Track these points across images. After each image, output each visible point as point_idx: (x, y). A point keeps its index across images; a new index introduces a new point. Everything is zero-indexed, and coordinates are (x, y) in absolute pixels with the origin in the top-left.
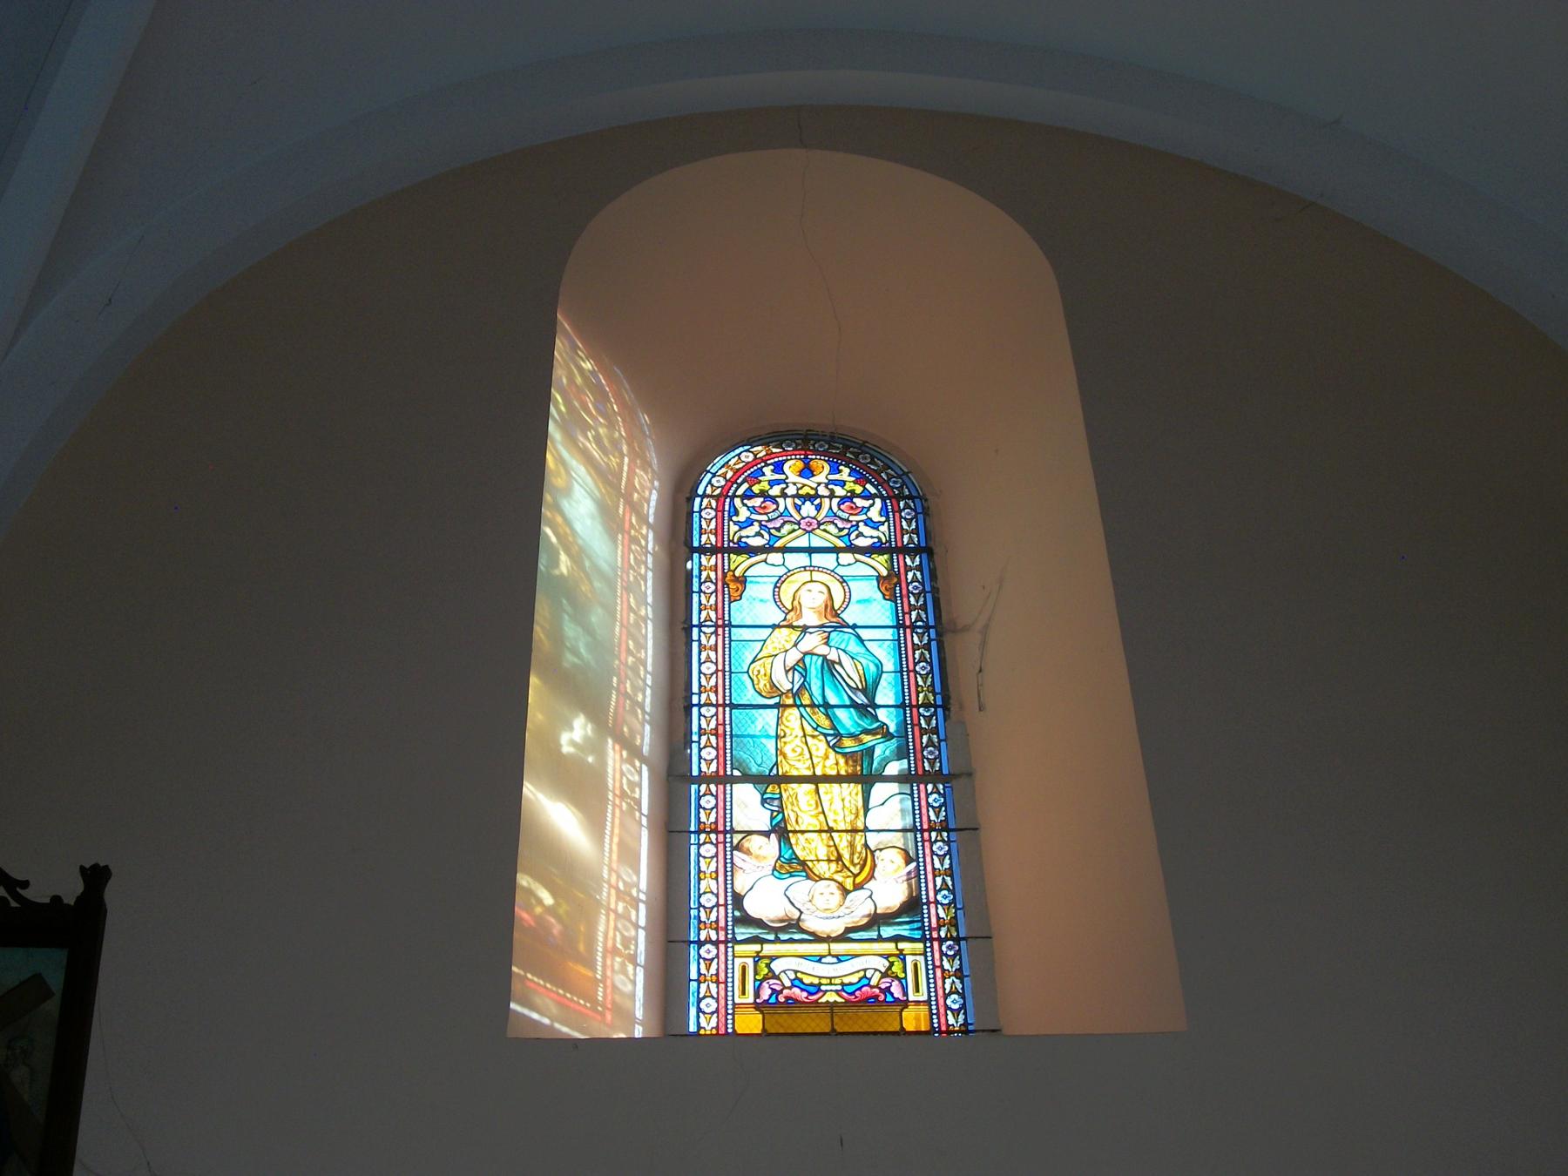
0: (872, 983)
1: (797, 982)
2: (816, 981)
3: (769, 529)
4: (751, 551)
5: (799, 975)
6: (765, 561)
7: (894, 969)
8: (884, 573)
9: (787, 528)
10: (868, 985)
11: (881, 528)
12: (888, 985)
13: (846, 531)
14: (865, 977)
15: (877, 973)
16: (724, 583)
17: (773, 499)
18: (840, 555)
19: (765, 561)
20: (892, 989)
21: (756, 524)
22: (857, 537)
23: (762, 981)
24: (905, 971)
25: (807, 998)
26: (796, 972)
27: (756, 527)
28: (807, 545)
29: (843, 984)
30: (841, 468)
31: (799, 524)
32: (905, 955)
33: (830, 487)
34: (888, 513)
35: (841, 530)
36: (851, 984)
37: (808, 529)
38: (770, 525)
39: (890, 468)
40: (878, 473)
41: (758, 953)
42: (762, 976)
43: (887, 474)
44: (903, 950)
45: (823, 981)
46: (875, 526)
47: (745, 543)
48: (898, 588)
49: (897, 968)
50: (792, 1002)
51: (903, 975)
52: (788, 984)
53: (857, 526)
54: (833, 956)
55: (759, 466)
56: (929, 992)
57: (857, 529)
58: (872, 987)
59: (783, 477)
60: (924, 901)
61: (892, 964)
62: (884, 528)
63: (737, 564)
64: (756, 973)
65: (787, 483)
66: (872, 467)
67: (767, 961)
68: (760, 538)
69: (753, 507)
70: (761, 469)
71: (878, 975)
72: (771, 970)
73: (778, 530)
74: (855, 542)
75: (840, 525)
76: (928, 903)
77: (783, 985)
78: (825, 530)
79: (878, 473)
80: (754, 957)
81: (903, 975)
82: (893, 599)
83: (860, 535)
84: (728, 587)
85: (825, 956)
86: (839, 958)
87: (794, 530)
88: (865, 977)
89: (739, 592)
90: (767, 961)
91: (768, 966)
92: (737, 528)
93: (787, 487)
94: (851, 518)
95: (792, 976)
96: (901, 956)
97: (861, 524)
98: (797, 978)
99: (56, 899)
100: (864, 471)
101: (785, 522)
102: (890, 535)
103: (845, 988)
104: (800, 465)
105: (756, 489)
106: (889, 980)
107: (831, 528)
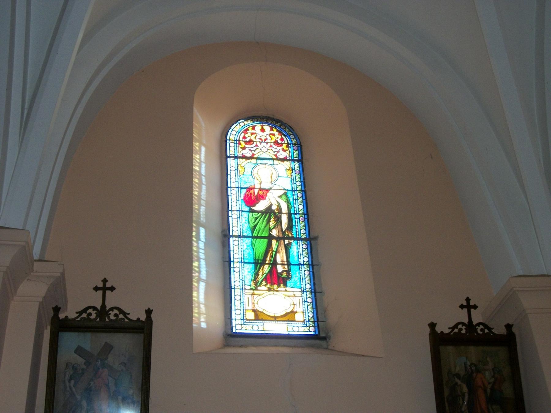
35: (274, 152)
38: (252, 149)
46: (285, 151)
73: (255, 151)
78: (269, 152)
93: (257, 135)
99: (442, 332)
100: (282, 131)
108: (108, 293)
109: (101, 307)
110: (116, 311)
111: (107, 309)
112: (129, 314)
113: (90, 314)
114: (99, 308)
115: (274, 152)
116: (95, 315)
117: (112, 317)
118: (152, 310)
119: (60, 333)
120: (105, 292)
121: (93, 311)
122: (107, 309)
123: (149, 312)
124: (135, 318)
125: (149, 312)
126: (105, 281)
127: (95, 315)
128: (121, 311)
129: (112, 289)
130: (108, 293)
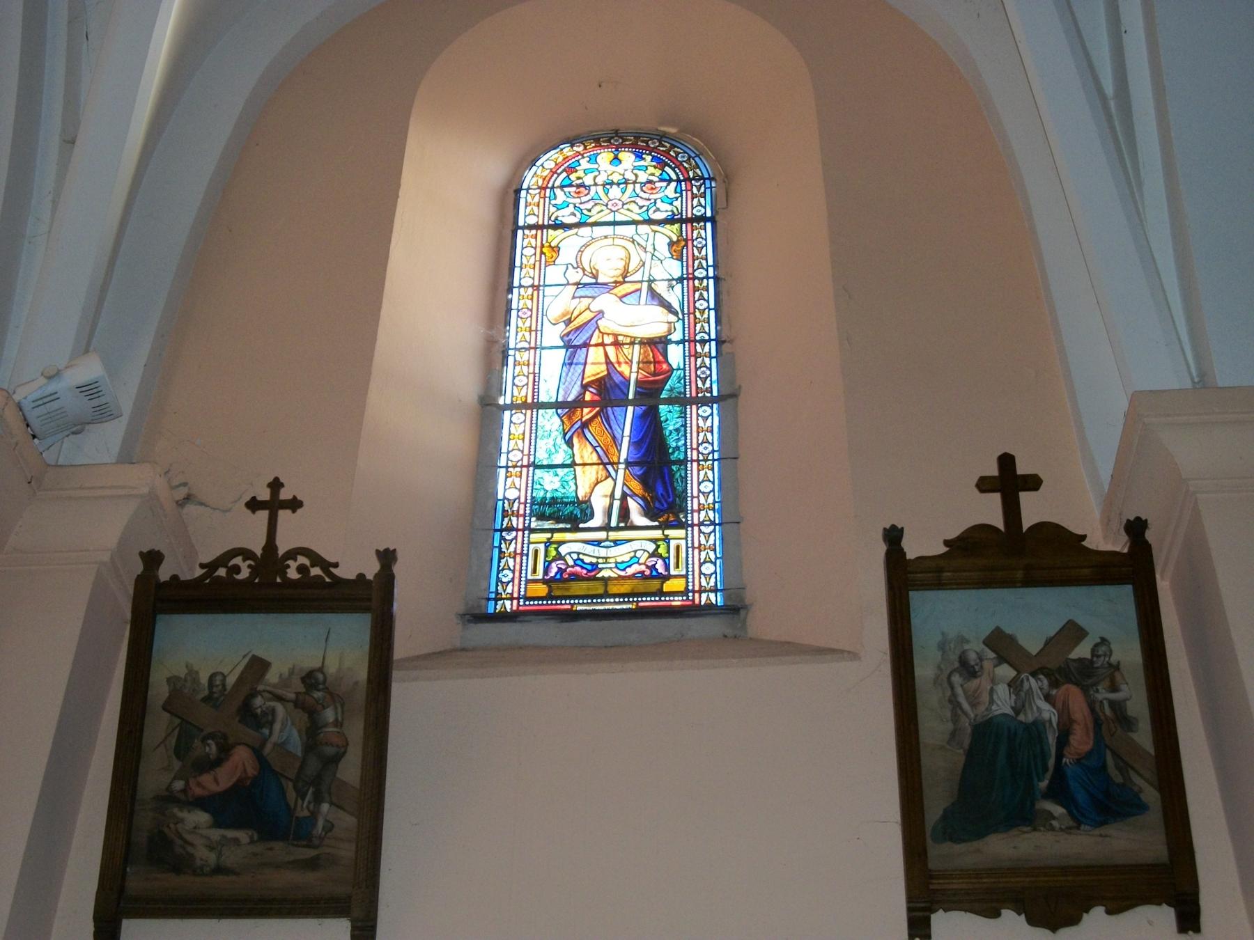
0: (640, 562)
1: (579, 562)
2: (594, 560)
3: (581, 210)
4: (566, 227)
5: (581, 556)
6: (576, 234)
7: (660, 551)
8: (675, 239)
9: (598, 208)
10: (638, 563)
11: (675, 203)
12: (654, 563)
13: (645, 208)
14: (635, 556)
15: (646, 553)
16: (542, 253)
17: (587, 188)
18: (639, 226)
19: (576, 234)
20: (657, 566)
21: (571, 206)
22: (655, 212)
23: (550, 563)
24: (668, 552)
25: (586, 574)
26: (578, 554)
27: (571, 208)
28: (613, 220)
29: (616, 563)
30: (644, 156)
31: (607, 205)
32: (669, 539)
33: (635, 171)
34: (682, 191)
35: (641, 207)
36: (623, 562)
37: (614, 209)
38: (582, 207)
39: (676, 147)
40: (668, 152)
41: (549, 539)
42: (551, 558)
43: (675, 152)
44: (668, 535)
45: (600, 561)
47: (561, 221)
48: (685, 251)
49: (662, 550)
50: (575, 577)
51: (667, 555)
52: (571, 562)
53: (655, 202)
54: (611, 541)
55: (577, 159)
56: (687, 568)
57: (655, 205)
58: (640, 564)
59: (596, 166)
60: (689, 495)
61: (658, 547)
62: (677, 203)
63: (553, 237)
64: (546, 556)
65: (599, 171)
66: (661, 149)
67: (556, 546)
68: (573, 217)
69: (569, 193)
70: (578, 161)
71: (646, 555)
72: (558, 553)
74: (651, 217)
75: (641, 203)
76: (692, 497)
77: (567, 564)
78: (628, 210)
79: (668, 152)
80: (545, 543)
81: (667, 555)
82: (681, 259)
83: (658, 210)
84: (545, 256)
85: (604, 541)
86: (616, 543)
87: (602, 211)
88: (635, 556)
89: (553, 259)
90: (556, 546)
91: (556, 549)
92: (555, 209)
94: (651, 197)
95: (575, 556)
96: (667, 539)
97: (658, 201)
98: (579, 559)
101: (596, 204)
102: (682, 211)
103: (618, 565)
104: (612, 156)
105: (573, 177)
106: (655, 559)
107: (633, 207)
108: (284, 515)
109: (264, 549)
110: (302, 560)
111: (281, 552)
112: (336, 565)
113: (237, 569)
114: (259, 552)
115: (641, 207)
116: (249, 570)
117: (293, 574)
118: (395, 550)
119: (159, 617)
120: (276, 516)
121: (244, 560)
122: (281, 552)
123: (387, 558)
124: (351, 575)
125: (387, 558)
126: (276, 485)
127: (249, 570)
128: (317, 560)
129: (295, 504)
130: (284, 515)
